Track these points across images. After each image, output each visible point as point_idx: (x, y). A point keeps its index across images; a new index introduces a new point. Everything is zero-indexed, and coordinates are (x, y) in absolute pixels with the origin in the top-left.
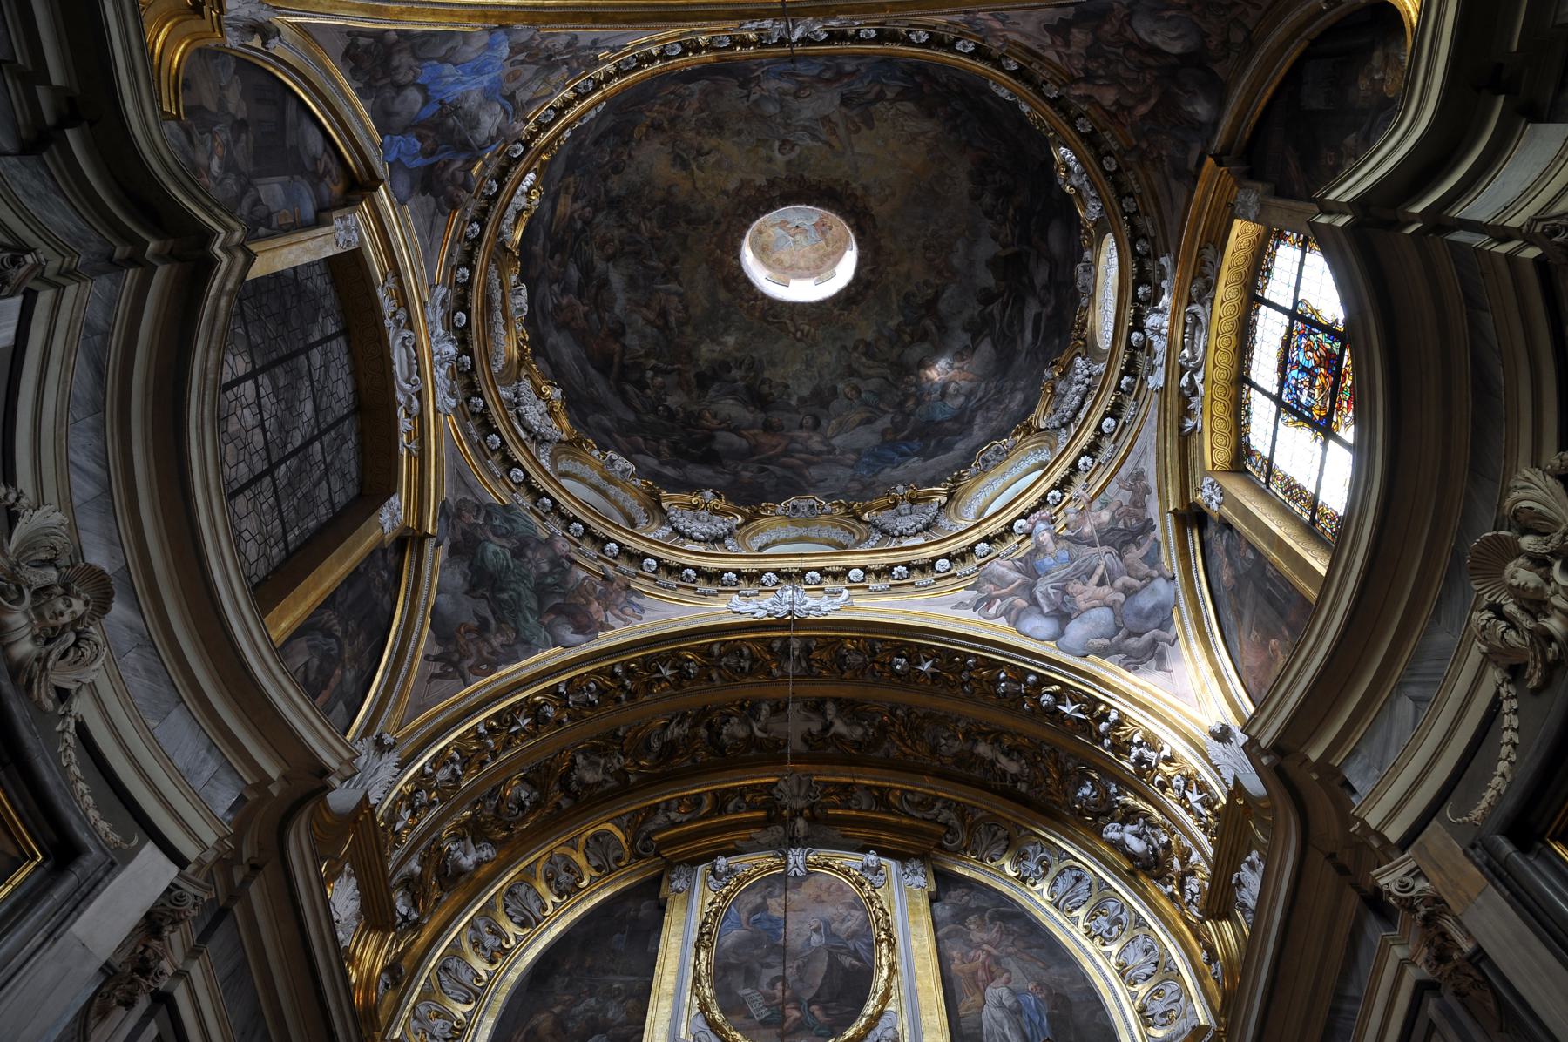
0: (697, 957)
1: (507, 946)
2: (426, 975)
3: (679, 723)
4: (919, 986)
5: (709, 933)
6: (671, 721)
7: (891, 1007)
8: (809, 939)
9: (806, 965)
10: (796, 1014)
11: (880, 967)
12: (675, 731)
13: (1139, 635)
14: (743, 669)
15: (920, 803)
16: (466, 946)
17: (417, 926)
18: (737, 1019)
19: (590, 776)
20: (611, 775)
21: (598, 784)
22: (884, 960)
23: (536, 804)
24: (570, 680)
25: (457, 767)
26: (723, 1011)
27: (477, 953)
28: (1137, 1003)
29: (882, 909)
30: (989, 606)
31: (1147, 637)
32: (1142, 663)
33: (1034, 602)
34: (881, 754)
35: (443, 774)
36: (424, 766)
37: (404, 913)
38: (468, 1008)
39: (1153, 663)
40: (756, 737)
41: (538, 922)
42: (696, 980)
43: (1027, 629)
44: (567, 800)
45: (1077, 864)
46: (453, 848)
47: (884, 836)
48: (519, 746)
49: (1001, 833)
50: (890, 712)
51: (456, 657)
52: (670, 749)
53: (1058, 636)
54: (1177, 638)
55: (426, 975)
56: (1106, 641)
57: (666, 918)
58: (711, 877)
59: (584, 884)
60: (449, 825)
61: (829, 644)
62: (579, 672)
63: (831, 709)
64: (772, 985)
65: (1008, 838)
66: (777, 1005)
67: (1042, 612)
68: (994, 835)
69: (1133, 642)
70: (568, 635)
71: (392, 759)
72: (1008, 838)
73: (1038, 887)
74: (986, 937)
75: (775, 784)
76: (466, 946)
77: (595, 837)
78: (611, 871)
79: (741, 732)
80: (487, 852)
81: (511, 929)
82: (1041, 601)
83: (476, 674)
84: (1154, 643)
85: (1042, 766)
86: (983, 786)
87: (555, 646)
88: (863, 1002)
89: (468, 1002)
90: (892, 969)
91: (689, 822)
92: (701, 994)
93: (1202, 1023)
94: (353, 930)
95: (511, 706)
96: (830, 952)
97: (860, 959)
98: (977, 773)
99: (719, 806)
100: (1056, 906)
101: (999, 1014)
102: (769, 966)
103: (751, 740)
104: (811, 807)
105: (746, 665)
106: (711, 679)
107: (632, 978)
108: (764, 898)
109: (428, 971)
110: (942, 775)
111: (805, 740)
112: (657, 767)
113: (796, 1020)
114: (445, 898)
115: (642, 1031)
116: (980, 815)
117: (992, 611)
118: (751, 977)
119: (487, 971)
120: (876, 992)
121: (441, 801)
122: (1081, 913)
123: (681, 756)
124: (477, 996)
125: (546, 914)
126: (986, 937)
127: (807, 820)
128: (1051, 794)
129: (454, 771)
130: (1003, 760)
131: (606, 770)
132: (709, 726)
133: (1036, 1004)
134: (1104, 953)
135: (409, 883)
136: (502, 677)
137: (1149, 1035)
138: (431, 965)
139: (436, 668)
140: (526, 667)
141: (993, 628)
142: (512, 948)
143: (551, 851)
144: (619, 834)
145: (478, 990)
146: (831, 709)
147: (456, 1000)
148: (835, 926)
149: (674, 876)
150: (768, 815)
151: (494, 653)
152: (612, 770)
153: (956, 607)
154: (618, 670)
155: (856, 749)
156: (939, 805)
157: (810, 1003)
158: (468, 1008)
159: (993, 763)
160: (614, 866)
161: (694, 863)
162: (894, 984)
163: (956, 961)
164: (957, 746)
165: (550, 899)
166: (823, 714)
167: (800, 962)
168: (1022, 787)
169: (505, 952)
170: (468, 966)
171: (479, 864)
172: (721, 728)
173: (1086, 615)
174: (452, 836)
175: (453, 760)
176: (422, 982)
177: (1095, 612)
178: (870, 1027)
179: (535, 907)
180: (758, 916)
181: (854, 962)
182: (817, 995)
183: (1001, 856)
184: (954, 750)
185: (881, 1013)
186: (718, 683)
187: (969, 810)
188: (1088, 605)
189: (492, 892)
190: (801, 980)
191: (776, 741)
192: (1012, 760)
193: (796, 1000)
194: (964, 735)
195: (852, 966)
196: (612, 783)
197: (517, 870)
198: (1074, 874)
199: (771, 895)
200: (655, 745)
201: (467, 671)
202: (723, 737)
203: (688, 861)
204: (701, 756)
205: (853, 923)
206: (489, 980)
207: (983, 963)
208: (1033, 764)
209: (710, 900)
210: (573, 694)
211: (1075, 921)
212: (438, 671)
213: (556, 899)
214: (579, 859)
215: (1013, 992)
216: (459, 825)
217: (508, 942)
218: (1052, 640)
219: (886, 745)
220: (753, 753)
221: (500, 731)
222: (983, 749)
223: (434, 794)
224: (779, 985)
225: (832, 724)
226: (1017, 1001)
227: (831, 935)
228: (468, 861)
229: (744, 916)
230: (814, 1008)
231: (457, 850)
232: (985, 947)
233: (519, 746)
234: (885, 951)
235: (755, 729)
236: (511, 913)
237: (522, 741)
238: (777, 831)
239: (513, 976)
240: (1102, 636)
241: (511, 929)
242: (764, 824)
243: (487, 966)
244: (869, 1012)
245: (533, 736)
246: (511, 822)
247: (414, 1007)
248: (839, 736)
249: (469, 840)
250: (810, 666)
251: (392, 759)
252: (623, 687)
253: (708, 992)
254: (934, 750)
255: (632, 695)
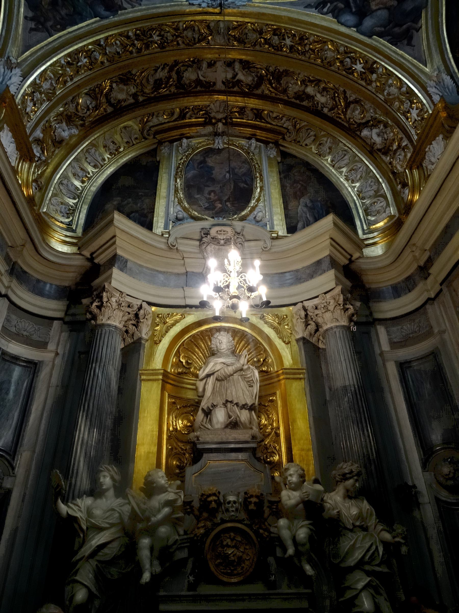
0: (176, 181)
1: (89, 176)
2: (53, 186)
3: (163, 69)
4: (272, 196)
5: (181, 172)
6: (159, 68)
7: (261, 204)
8: (225, 176)
9: (223, 186)
10: (220, 205)
11: (256, 188)
12: (161, 74)
13: (401, 26)
14: (194, 39)
15: (276, 118)
16: (70, 175)
17: (46, 163)
18: (195, 207)
19: (121, 96)
20: (130, 96)
21: (125, 101)
22: (258, 185)
23: (96, 108)
24: (106, 38)
25: (53, 82)
26: (188, 203)
27: (76, 178)
28: (364, 207)
29: (257, 164)
30: (324, 7)
31: (405, 27)
32: (399, 41)
33: (348, 5)
34: (259, 92)
35: (46, 86)
36: (35, 79)
37: (39, 155)
38: (75, 201)
39: (405, 42)
40: (200, 80)
41: (102, 166)
42: (176, 191)
43: (343, 21)
44: (110, 108)
45: (346, 148)
46: (57, 126)
47: (258, 132)
48: (83, 75)
49: (312, 133)
50: (266, 69)
51: (42, 20)
52: (158, 84)
53: (358, 26)
54: (421, 27)
55: (53, 186)
56: (383, 29)
57: (160, 166)
58: (180, 148)
59: (122, 149)
60: (52, 114)
61: (239, 25)
62: (110, 33)
63: (237, 66)
64: (210, 194)
65: (315, 136)
66: (212, 202)
67: (351, 12)
68: (309, 134)
69: (397, 30)
70: (101, 10)
71: (17, 71)
72: (315, 136)
73: (327, 158)
74: (301, 178)
75: (209, 106)
76: (70, 175)
77: (125, 127)
78: (134, 145)
79: (193, 77)
80: (75, 131)
81: (90, 169)
82: (352, 4)
83: (55, 31)
84: (408, 30)
85: (337, 99)
86: (306, 109)
87: (95, 17)
88: (249, 201)
89: (74, 199)
90: (261, 188)
91: (168, 122)
92: (179, 197)
93: (393, 214)
94: (15, 159)
95: (76, 50)
96: (234, 182)
97: (247, 184)
98: (305, 103)
99: (182, 116)
100: (333, 166)
101: (305, 209)
102: (208, 186)
103: (198, 82)
104: (225, 118)
105: (196, 36)
106: (178, 44)
107: (147, 191)
108: (205, 158)
109: (54, 184)
110: (287, 103)
111: (223, 82)
112: (152, 93)
113: (220, 208)
114: (57, 151)
115: (154, 212)
116: (304, 124)
117: (325, 10)
118: (200, 191)
119: (81, 186)
120: (254, 198)
121: (48, 100)
122: (344, 170)
123: (164, 88)
124: (79, 197)
125: (106, 162)
126: (301, 178)
127: (224, 124)
128: (339, 114)
129: (51, 83)
130: (318, 95)
131: (127, 93)
132: (178, 73)
133: (321, 206)
134: (353, 187)
135: (38, 141)
136: (69, 33)
137: (368, 219)
138: (55, 181)
139: (32, 25)
140: (82, 28)
141: (325, 20)
142: (91, 177)
143: (104, 133)
144: (136, 127)
145: (79, 194)
146: (237, 66)
147: (69, 198)
148: (236, 170)
149: (163, 147)
150: (205, 121)
151: (62, 18)
152: (130, 93)
153: (306, 7)
154: (130, 34)
155: (248, 89)
156: (284, 119)
157: (226, 201)
158: (75, 201)
159: (313, 97)
160: (134, 143)
161: (172, 142)
162: (262, 195)
163: (288, 188)
164: (297, 88)
165: (107, 156)
166: (234, 70)
167: (221, 185)
168: (326, 110)
169: (89, 179)
170: (73, 184)
171: (71, 136)
172: (183, 73)
173: (374, 14)
174: (55, 120)
175: (51, 78)
176: (52, 189)
177: (379, 12)
178: (251, 211)
179: (99, 159)
180: (202, 165)
181: (245, 186)
182: (229, 198)
183: (311, 144)
184: (295, 91)
185: (256, 206)
186: (182, 46)
187: (299, 121)
188: (377, 7)
189: (79, 150)
190: (222, 192)
191: (209, 83)
192: (323, 96)
193: (220, 200)
194: (301, 82)
195: (244, 187)
196: (131, 101)
197: (89, 141)
198: (344, 152)
199: (207, 156)
200: (152, 81)
201: (49, 28)
202: (184, 78)
203: (168, 141)
204: (173, 89)
205: (244, 170)
206: (83, 190)
207: (300, 189)
208: (333, 98)
209: (180, 158)
210: (108, 46)
211: (341, 173)
212: (33, 26)
213: (109, 156)
214: (117, 138)
215: (311, 201)
216: (58, 115)
217: (89, 174)
218: (354, 27)
219: (263, 87)
220: (199, 88)
221: (72, 64)
222: (310, 90)
223: (43, 95)
224: (212, 194)
225: (237, 74)
226: (313, 204)
227: (235, 174)
228: (65, 134)
229: (196, 165)
230: (227, 203)
231: (59, 127)
232: (301, 182)
233: (83, 75)
234: (258, 181)
235: (200, 76)
236: (89, 161)
237: (85, 72)
238: (209, 129)
239: (94, 189)
240: (381, 26)
241: (90, 169)
242: (203, 125)
243: (81, 184)
244: (252, 205)
245: (90, 69)
246: (84, 117)
247: (50, 199)
248: (239, 81)
249: (64, 124)
250: (229, 39)
251: (17, 71)
252: (133, 45)
253: (181, 196)
254: (285, 91)
255: (139, 51)
